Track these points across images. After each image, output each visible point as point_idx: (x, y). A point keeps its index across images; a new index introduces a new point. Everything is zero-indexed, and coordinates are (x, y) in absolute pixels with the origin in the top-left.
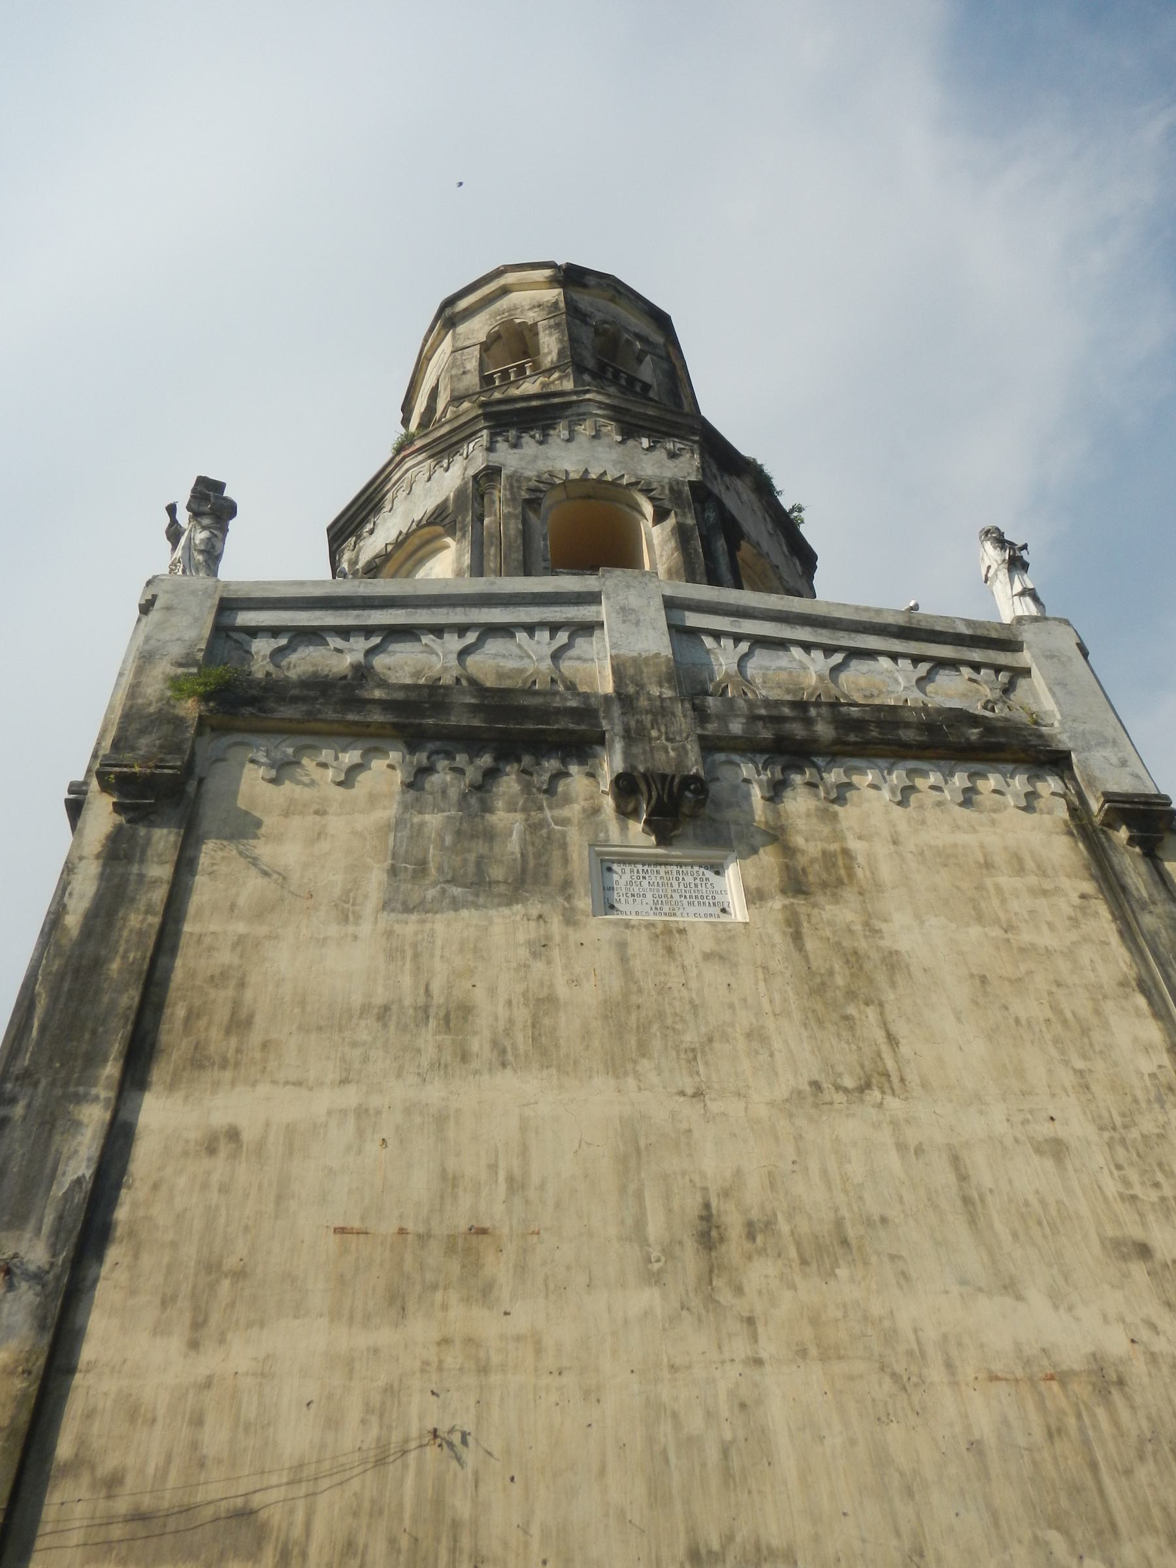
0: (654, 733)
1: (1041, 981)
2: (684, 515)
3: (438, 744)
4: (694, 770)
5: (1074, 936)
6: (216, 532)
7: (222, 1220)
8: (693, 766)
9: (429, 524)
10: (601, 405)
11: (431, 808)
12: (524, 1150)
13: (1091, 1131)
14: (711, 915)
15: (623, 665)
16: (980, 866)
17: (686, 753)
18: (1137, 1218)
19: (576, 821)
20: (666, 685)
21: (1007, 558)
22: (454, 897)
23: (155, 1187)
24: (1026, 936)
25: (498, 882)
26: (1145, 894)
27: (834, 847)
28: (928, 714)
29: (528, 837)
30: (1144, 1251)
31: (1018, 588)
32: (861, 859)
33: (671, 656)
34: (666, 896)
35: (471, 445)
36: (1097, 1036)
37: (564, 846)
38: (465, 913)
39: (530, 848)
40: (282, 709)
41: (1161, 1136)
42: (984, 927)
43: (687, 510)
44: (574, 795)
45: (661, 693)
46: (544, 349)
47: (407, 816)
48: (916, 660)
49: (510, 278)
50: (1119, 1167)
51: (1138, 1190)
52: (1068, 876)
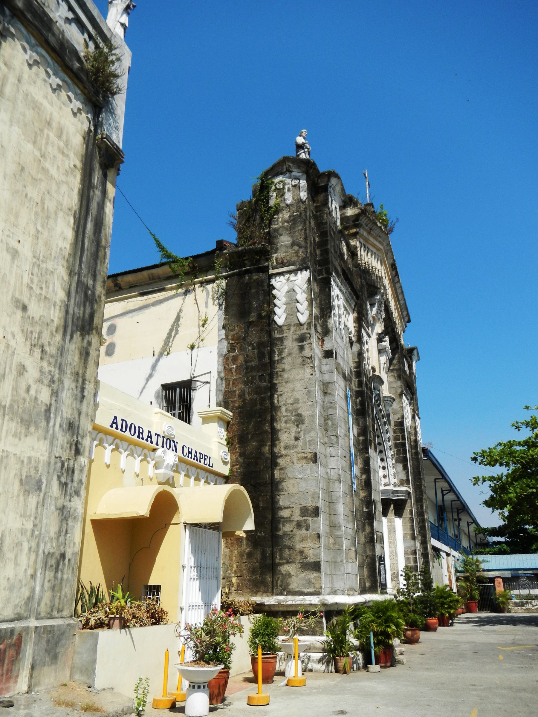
1: (43, 186)
5: (63, 178)
13: (30, 255)
18: (29, 296)
24: (47, 165)
26: (96, 183)
30: (25, 308)
36: (51, 222)
41: (52, 272)
50: (32, 274)
51: (34, 286)
52: (74, 154)
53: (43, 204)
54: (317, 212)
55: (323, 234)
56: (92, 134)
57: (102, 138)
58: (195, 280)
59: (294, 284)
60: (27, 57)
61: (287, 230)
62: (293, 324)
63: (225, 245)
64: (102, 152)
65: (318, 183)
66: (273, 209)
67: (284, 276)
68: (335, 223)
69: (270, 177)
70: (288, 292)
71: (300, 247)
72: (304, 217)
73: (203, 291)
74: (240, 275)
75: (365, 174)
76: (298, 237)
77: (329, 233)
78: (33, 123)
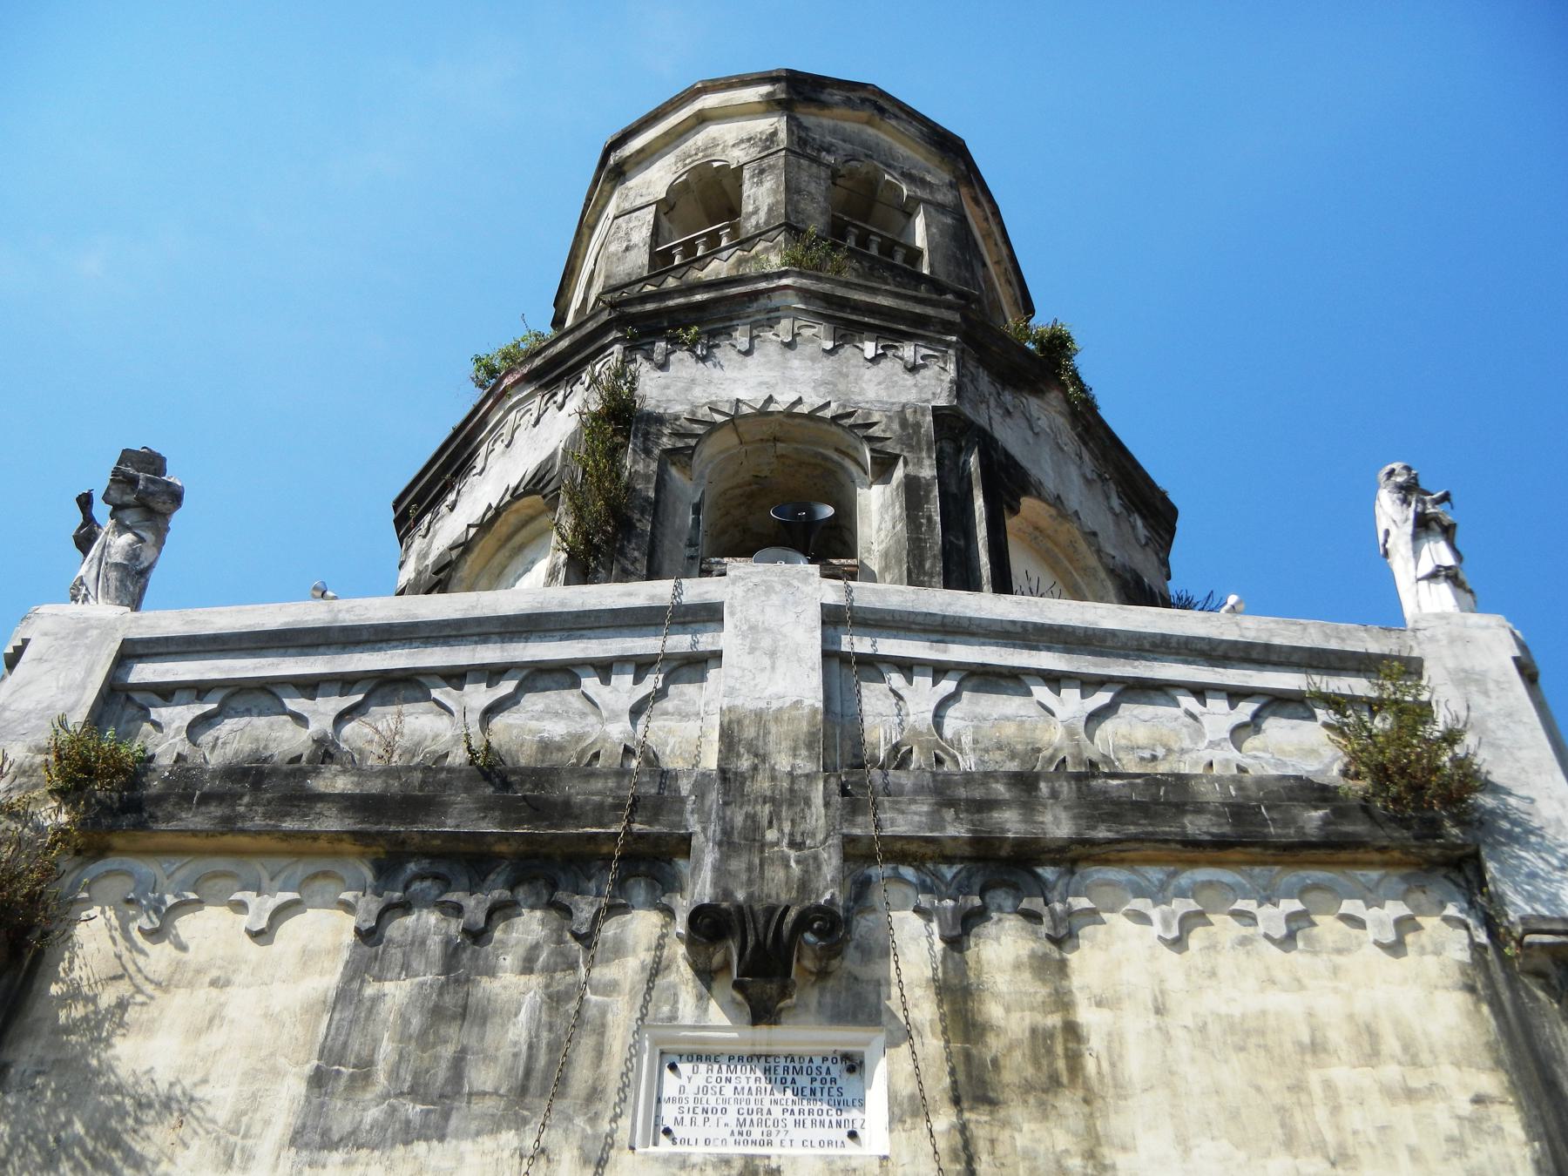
0: (771, 835)
2: (919, 463)
3: (425, 863)
4: (827, 896)
6: (143, 534)
8: (826, 888)
9: (527, 493)
10: (804, 294)
11: (398, 970)
14: (830, 1143)
15: (739, 722)
16: (1301, 1048)
17: (819, 868)
19: (626, 986)
20: (804, 753)
21: (1412, 516)
22: (408, 1122)
25: (484, 1094)
27: (1054, 1020)
28: (1241, 787)
29: (544, 1018)
31: (1426, 567)
32: (1096, 1042)
33: (820, 705)
34: (760, 1111)
35: (598, 367)
37: (601, 1030)
38: (420, 1147)
39: (545, 1035)
40: (184, 815)
42: (1296, 1157)
43: (924, 454)
44: (630, 942)
45: (793, 767)
46: (747, 207)
47: (355, 985)
48: (1235, 695)
49: (709, 101)
52: (1457, 1064)
56: (1491, 955)
60: (1157, 929)
64: (1555, 982)
78: (1258, 1089)
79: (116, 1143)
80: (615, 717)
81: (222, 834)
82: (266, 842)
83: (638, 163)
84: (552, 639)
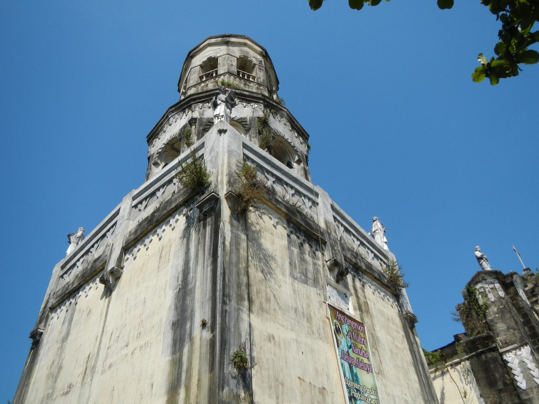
7: (276, 365)
9: (236, 121)
12: (328, 368)
23: (261, 348)
24: (396, 343)
27: (365, 300)
32: (370, 307)
53: (403, 366)
54: (513, 301)
55: (525, 316)
56: (400, 312)
57: (407, 314)
58: (447, 364)
59: (521, 357)
60: (372, 290)
61: (499, 319)
62: (533, 387)
63: (460, 337)
65: (505, 282)
66: (484, 307)
67: (511, 352)
68: (527, 304)
69: (472, 286)
70: (519, 363)
71: (515, 329)
72: (508, 308)
73: (455, 371)
74: (478, 355)
75: (514, 250)
76: (510, 323)
77: (528, 314)
79: (268, 263)
80: (308, 208)
81: (269, 201)
82: (273, 207)
83: (231, 44)
84: (298, 185)
